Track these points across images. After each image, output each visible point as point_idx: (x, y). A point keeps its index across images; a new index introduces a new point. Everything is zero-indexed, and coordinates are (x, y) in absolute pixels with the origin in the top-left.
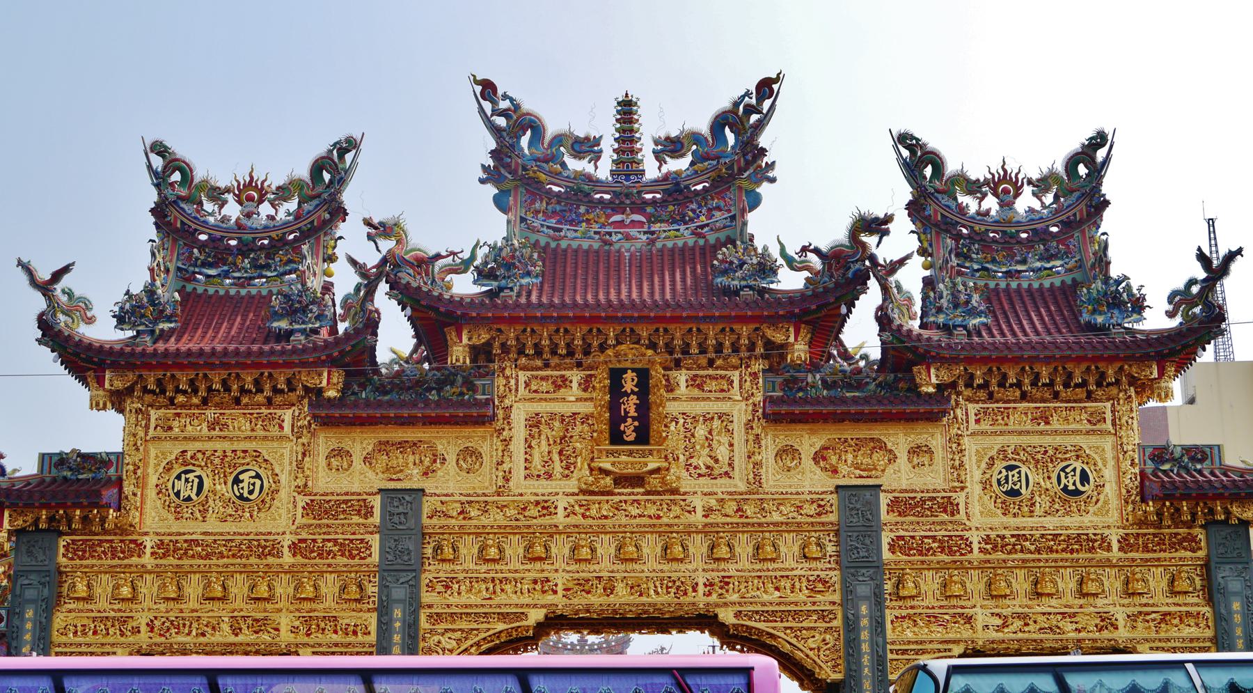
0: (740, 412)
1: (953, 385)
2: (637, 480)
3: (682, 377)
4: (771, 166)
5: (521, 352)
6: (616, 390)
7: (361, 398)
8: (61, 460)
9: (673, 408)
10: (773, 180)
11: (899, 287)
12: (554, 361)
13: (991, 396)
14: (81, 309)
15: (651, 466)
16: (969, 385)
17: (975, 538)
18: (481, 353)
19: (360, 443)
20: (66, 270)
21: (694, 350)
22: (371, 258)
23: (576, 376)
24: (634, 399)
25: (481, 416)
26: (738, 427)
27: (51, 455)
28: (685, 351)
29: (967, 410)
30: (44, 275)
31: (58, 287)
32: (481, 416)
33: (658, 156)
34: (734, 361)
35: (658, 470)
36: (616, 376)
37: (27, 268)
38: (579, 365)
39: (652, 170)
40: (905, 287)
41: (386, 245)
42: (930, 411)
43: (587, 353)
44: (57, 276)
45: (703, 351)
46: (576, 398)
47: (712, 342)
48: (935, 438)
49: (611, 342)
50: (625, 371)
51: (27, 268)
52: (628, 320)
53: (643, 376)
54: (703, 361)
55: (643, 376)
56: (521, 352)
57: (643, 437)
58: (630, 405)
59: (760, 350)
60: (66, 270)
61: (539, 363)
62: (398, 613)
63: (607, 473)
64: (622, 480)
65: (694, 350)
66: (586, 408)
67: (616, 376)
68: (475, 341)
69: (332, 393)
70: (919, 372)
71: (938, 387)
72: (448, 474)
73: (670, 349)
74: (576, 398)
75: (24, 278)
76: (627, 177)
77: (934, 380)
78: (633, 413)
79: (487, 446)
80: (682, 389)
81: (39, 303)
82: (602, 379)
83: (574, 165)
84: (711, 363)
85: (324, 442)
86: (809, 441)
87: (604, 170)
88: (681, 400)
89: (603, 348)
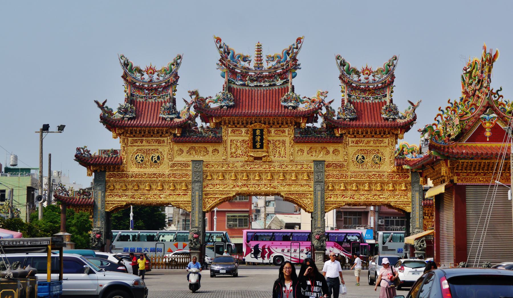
0: (288, 140)
1: (345, 133)
2: (260, 158)
3: (273, 130)
4: (299, 65)
5: (229, 123)
6: (254, 134)
7: (185, 134)
8: (105, 152)
9: (270, 138)
10: (300, 69)
11: (331, 108)
12: (238, 126)
13: (355, 137)
14: (110, 112)
15: (264, 155)
16: (349, 133)
17: (349, 174)
18: (218, 125)
19: (185, 148)
20: (105, 102)
21: (276, 124)
22: (189, 100)
23: (244, 130)
24: (259, 137)
25: (219, 140)
26: (287, 144)
27: (102, 150)
28: (274, 124)
29: (350, 140)
30: (101, 103)
31: (104, 106)
32: (219, 140)
33: (267, 61)
34: (286, 126)
35: (264, 156)
36: (254, 131)
37: (97, 102)
38: (245, 127)
39: (266, 66)
40: (333, 108)
41: (194, 97)
42: (339, 140)
43: (247, 123)
44: (104, 103)
45: (278, 124)
46: (243, 135)
47: (280, 122)
48: (340, 147)
49: (253, 122)
50: (257, 129)
51: (97, 102)
52: (258, 118)
53: (262, 131)
54: (278, 126)
55: (262, 131)
56: (229, 123)
57: (262, 147)
58: (258, 138)
59: (294, 123)
60: (105, 102)
61: (234, 126)
62: (197, 193)
63: (252, 156)
64: (256, 158)
65: (276, 124)
66: (247, 138)
67: (254, 131)
68: (217, 121)
69: (179, 135)
70: (336, 131)
71: (340, 134)
72: (211, 157)
73: (269, 124)
74: (243, 135)
75: (96, 105)
76: (259, 68)
77: (340, 133)
78: (259, 141)
79: (221, 148)
80: (273, 133)
81: (100, 111)
82: (250, 132)
83: (243, 63)
84: (280, 127)
85: (176, 147)
86: (306, 147)
87: (252, 66)
88: (273, 135)
89: (251, 124)
